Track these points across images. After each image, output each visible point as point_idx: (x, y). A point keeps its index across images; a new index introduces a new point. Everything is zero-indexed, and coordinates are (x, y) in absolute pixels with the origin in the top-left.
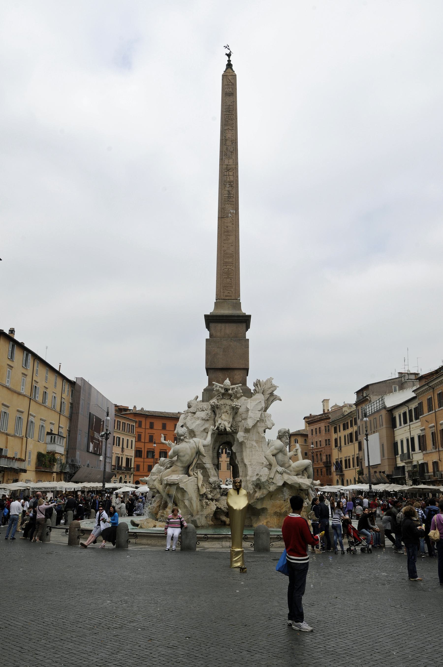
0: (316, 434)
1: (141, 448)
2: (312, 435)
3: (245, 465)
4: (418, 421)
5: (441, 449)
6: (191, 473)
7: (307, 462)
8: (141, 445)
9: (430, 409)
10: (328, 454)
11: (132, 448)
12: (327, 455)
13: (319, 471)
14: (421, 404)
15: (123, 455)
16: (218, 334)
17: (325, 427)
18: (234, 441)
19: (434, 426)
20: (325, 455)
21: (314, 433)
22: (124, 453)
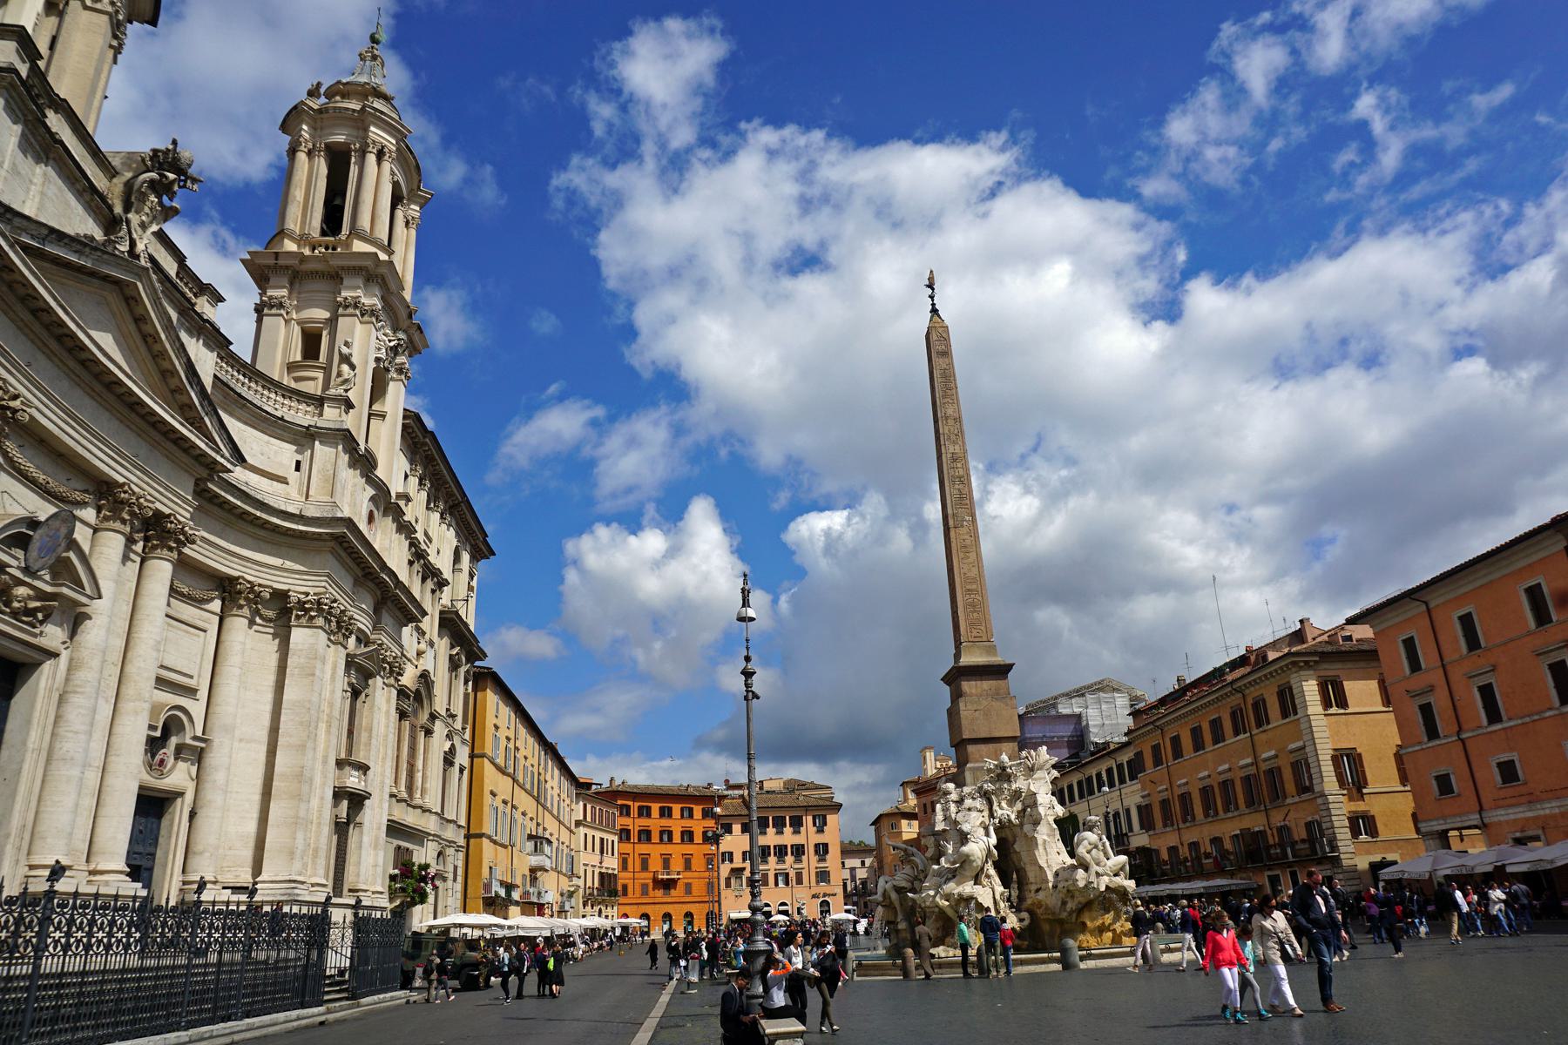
2: (926, 813)
3: (1040, 867)
5: (1181, 826)
7: (1123, 858)
9: (1158, 761)
14: (1139, 755)
16: (974, 691)
18: (1015, 837)
19: (1167, 789)
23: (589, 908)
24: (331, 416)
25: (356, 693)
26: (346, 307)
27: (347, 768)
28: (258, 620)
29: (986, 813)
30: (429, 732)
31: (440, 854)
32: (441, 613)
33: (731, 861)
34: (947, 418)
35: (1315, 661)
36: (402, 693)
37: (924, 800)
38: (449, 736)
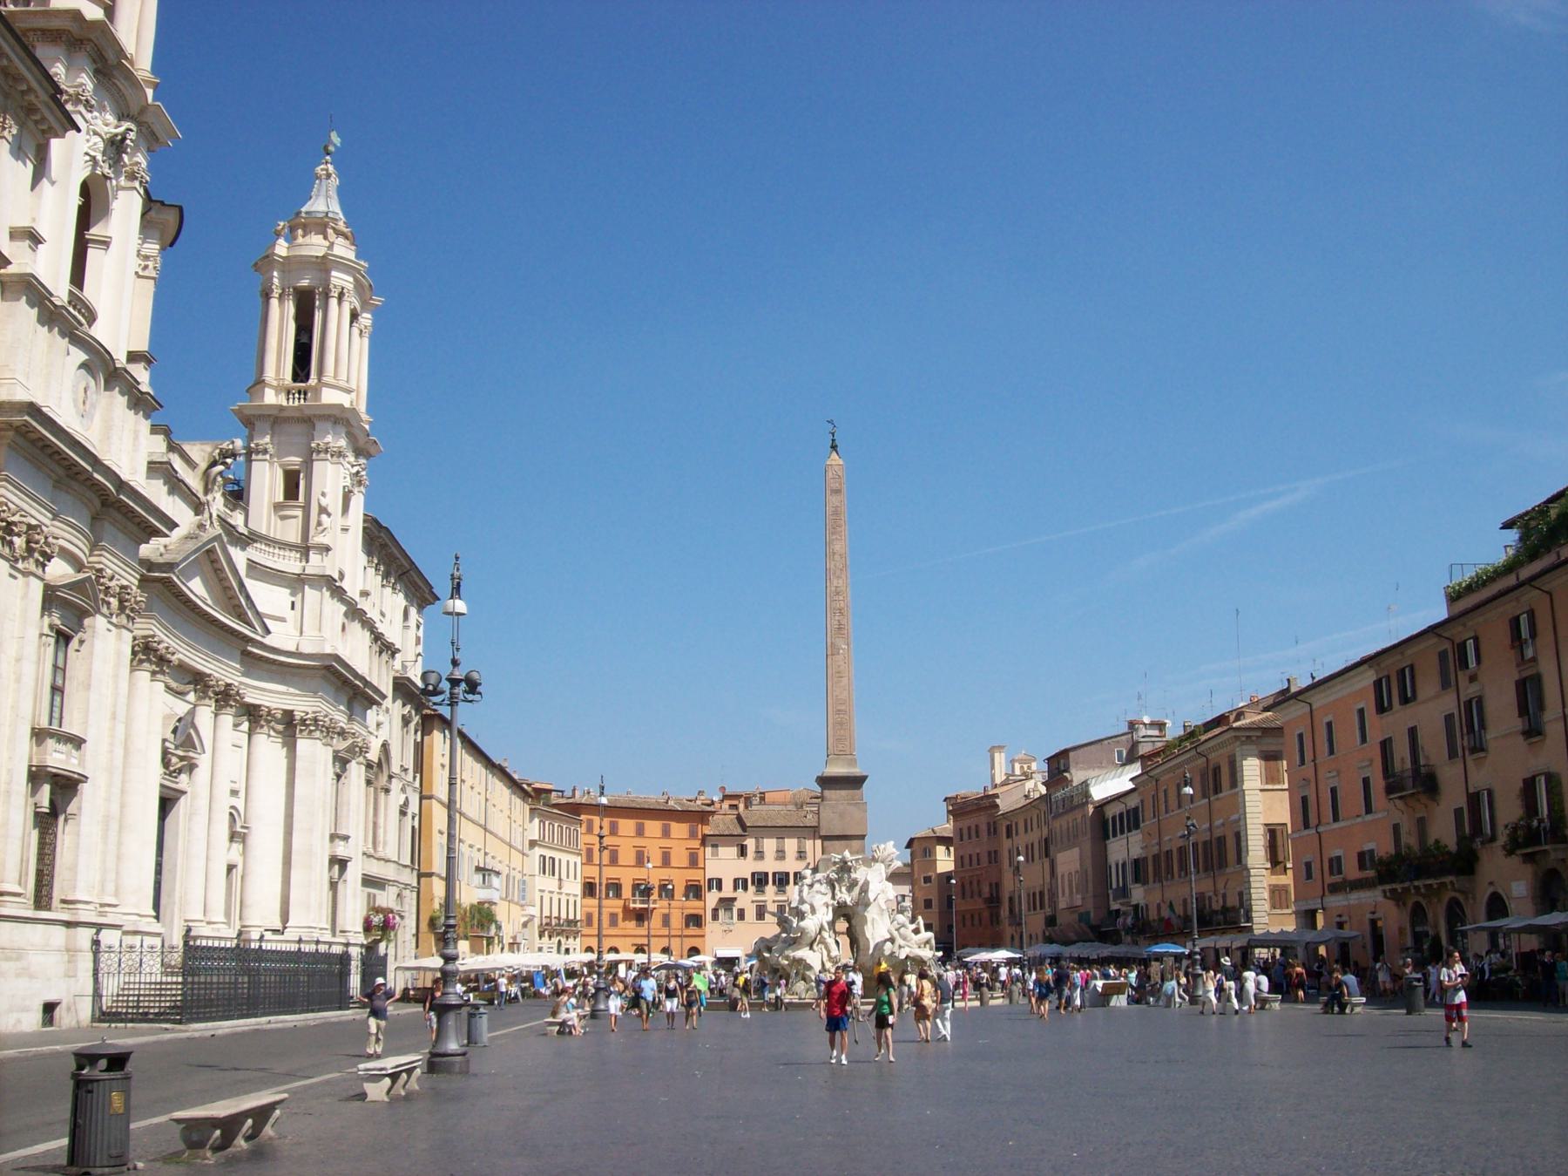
0: (970, 838)
1: (594, 878)
2: (962, 840)
4: (1138, 831)
6: (815, 947)
7: (930, 935)
8: (593, 872)
10: (994, 882)
11: (575, 878)
12: (991, 885)
13: (976, 917)
15: (561, 893)
17: (989, 824)
20: (988, 884)
21: (965, 837)
22: (562, 890)
23: (546, 938)
24: (316, 564)
25: (339, 777)
26: (319, 452)
27: (337, 840)
28: (272, 733)
29: (830, 895)
30: (387, 791)
31: (398, 895)
32: (395, 678)
33: (720, 888)
34: (834, 554)
35: (1257, 737)
36: (369, 766)
37: (960, 825)
38: (403, 790)
